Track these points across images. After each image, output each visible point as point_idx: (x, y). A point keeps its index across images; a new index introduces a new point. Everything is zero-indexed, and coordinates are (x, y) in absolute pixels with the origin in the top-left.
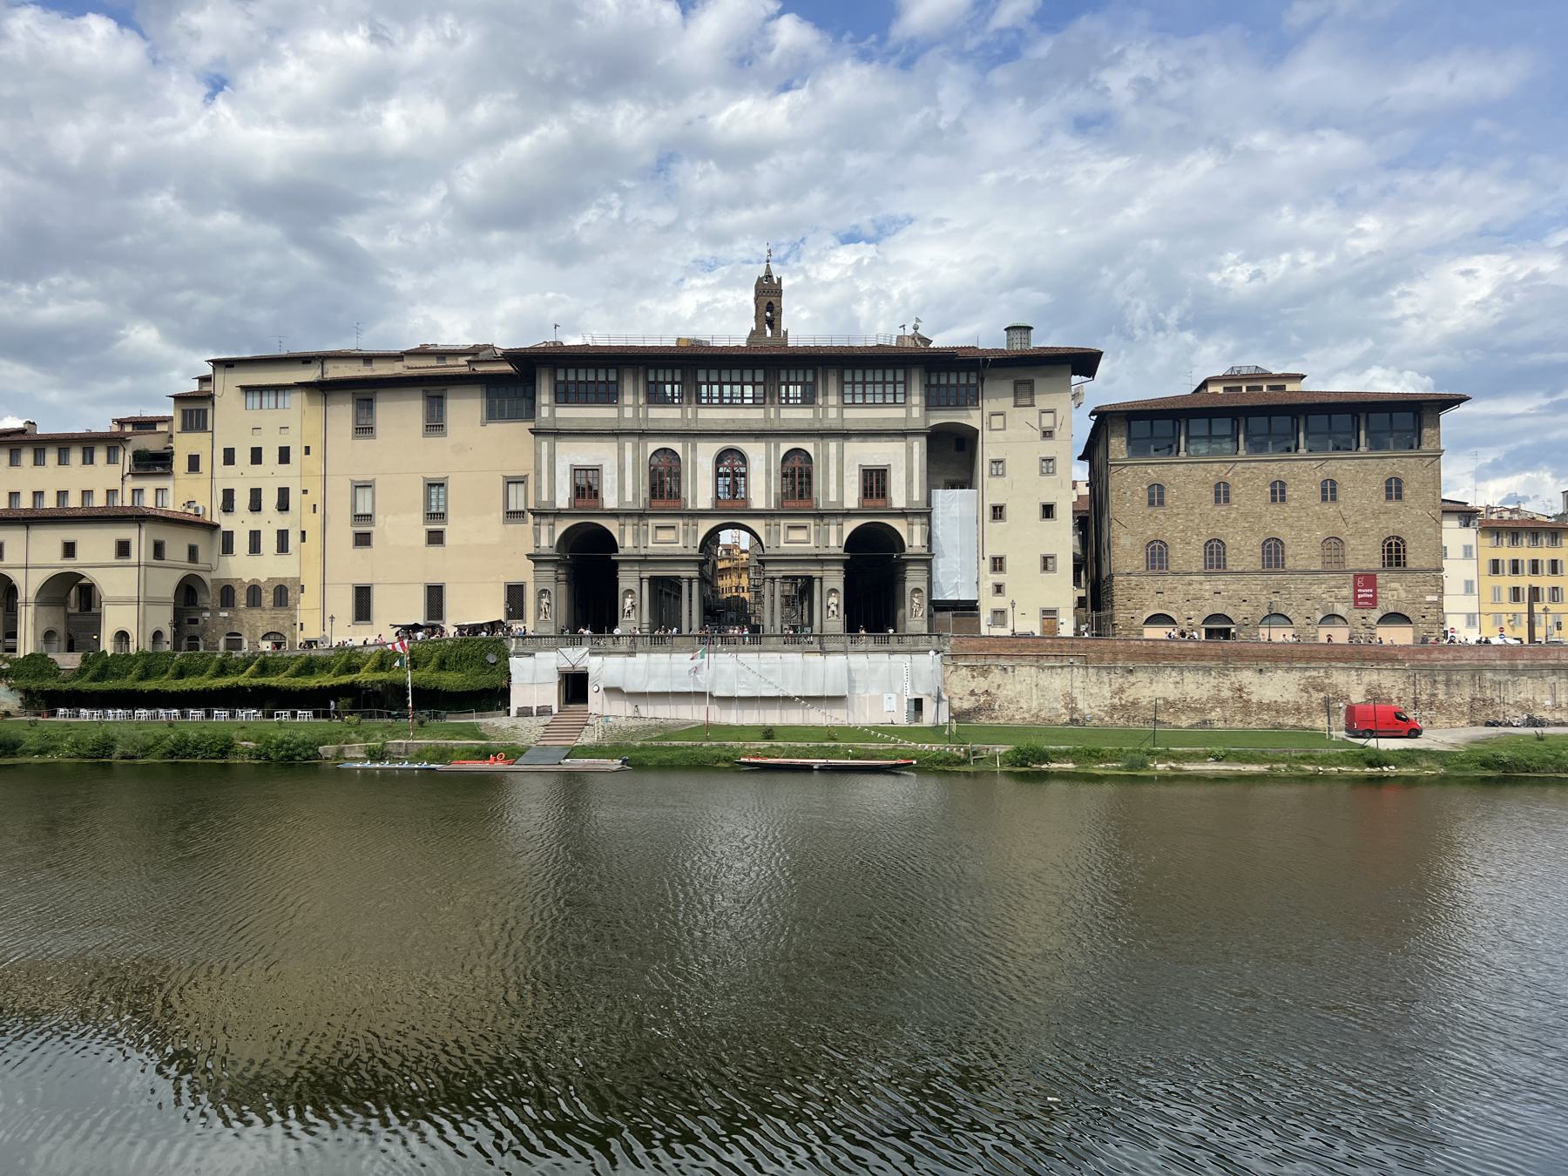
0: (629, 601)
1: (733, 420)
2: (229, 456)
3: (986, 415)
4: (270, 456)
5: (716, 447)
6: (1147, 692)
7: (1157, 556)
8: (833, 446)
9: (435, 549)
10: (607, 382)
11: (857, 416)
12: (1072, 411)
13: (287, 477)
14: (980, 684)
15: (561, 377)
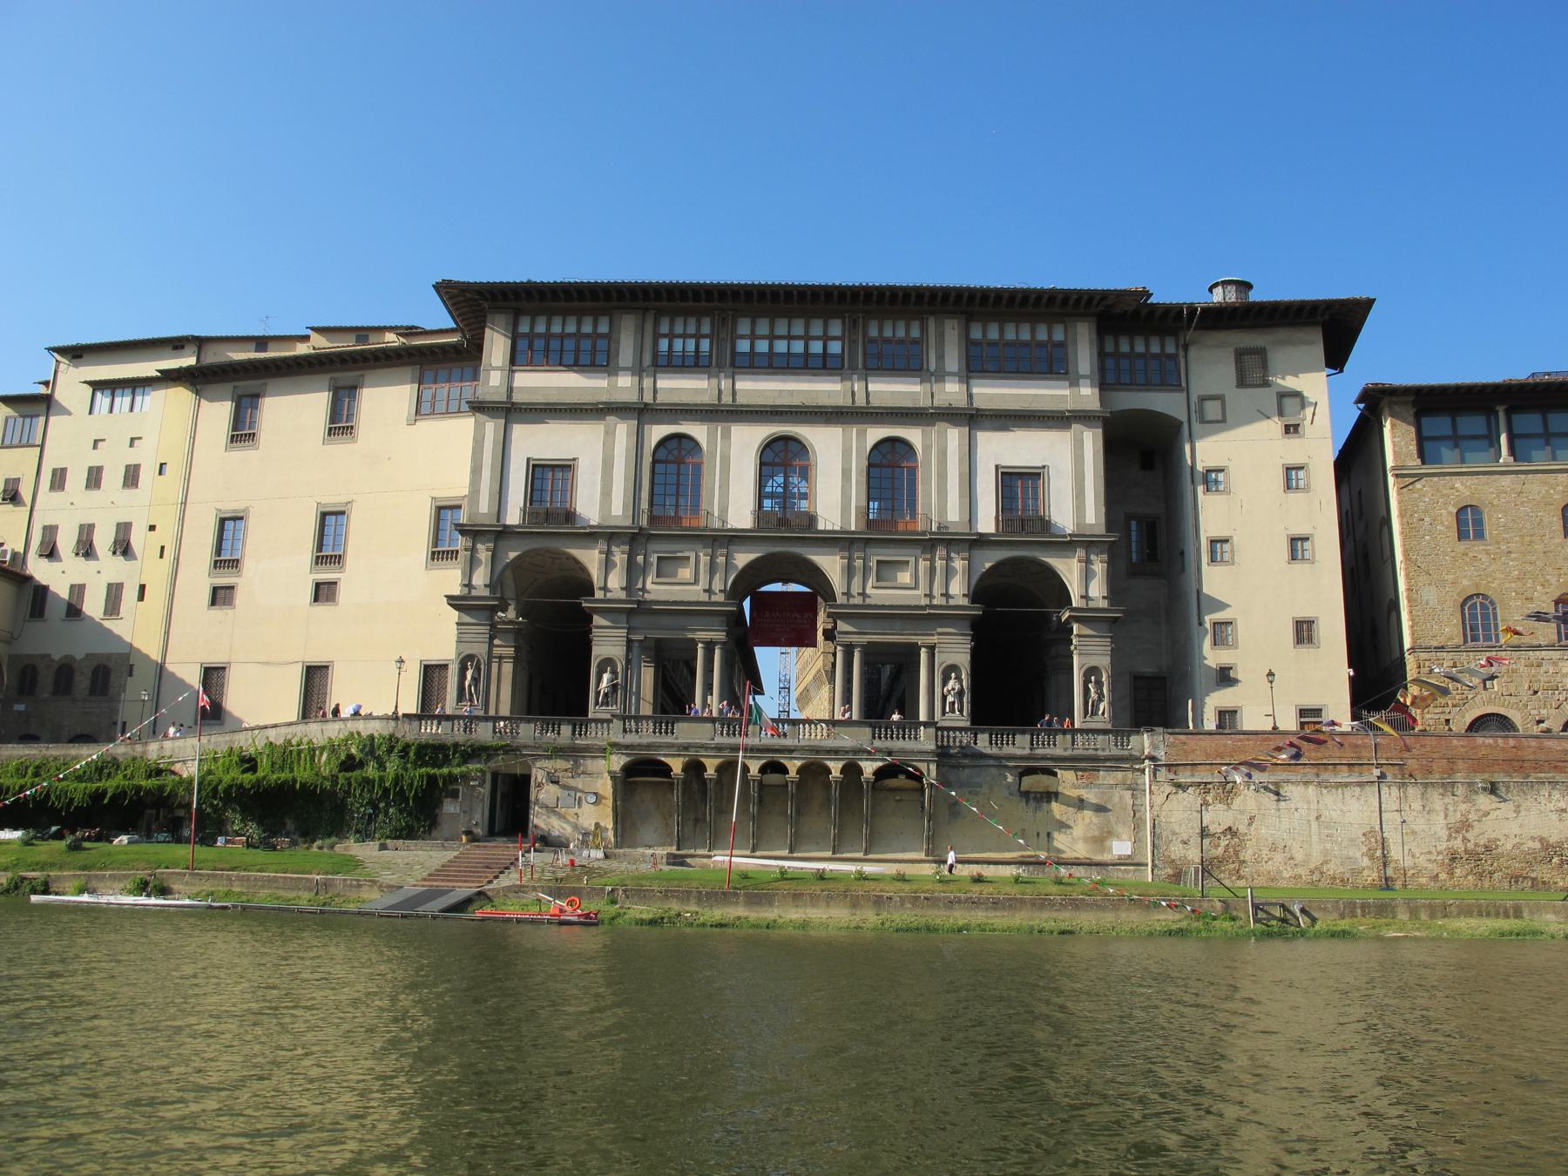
0: (606, 677)
1: (791, 392)
2: (59, 479)
3: (1194, 399)
4: (113, 478)
5: (759, 433)
6: (1513, 828)
7: (1477, 616)
8: (954, 436)
9: (322, 610)
10: (595, 336)
11: (992, 393)
12: (1324, 399)
13: (135, 507)
14: (1218, 818)
15: (524, 328)
